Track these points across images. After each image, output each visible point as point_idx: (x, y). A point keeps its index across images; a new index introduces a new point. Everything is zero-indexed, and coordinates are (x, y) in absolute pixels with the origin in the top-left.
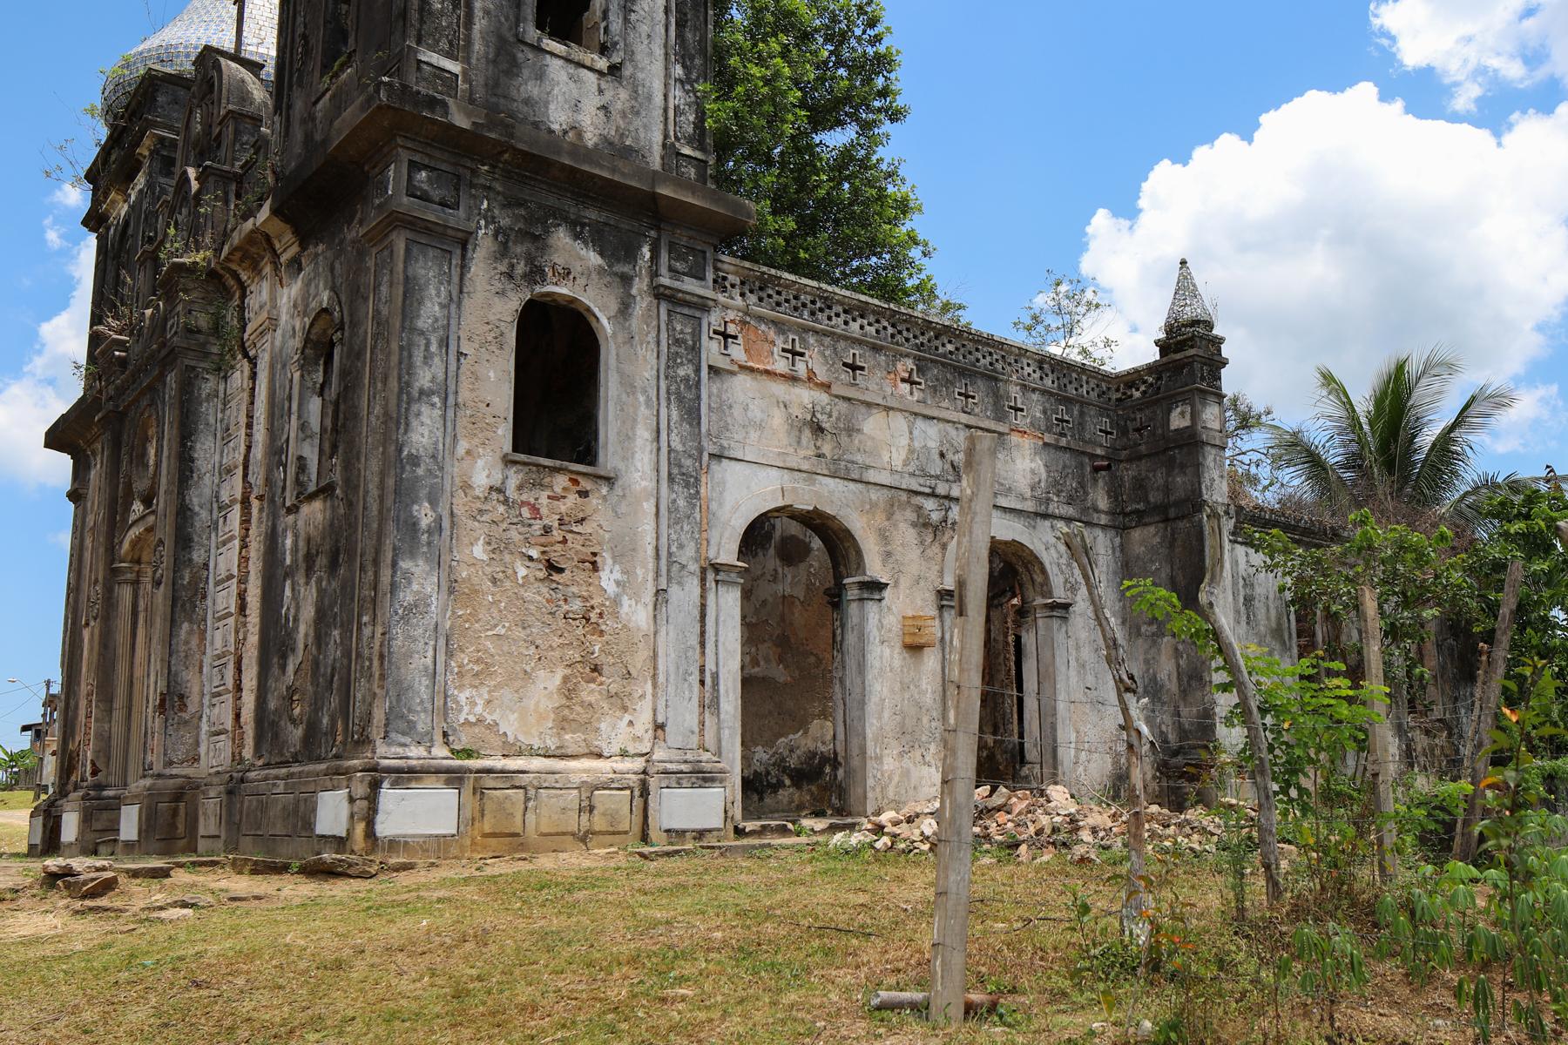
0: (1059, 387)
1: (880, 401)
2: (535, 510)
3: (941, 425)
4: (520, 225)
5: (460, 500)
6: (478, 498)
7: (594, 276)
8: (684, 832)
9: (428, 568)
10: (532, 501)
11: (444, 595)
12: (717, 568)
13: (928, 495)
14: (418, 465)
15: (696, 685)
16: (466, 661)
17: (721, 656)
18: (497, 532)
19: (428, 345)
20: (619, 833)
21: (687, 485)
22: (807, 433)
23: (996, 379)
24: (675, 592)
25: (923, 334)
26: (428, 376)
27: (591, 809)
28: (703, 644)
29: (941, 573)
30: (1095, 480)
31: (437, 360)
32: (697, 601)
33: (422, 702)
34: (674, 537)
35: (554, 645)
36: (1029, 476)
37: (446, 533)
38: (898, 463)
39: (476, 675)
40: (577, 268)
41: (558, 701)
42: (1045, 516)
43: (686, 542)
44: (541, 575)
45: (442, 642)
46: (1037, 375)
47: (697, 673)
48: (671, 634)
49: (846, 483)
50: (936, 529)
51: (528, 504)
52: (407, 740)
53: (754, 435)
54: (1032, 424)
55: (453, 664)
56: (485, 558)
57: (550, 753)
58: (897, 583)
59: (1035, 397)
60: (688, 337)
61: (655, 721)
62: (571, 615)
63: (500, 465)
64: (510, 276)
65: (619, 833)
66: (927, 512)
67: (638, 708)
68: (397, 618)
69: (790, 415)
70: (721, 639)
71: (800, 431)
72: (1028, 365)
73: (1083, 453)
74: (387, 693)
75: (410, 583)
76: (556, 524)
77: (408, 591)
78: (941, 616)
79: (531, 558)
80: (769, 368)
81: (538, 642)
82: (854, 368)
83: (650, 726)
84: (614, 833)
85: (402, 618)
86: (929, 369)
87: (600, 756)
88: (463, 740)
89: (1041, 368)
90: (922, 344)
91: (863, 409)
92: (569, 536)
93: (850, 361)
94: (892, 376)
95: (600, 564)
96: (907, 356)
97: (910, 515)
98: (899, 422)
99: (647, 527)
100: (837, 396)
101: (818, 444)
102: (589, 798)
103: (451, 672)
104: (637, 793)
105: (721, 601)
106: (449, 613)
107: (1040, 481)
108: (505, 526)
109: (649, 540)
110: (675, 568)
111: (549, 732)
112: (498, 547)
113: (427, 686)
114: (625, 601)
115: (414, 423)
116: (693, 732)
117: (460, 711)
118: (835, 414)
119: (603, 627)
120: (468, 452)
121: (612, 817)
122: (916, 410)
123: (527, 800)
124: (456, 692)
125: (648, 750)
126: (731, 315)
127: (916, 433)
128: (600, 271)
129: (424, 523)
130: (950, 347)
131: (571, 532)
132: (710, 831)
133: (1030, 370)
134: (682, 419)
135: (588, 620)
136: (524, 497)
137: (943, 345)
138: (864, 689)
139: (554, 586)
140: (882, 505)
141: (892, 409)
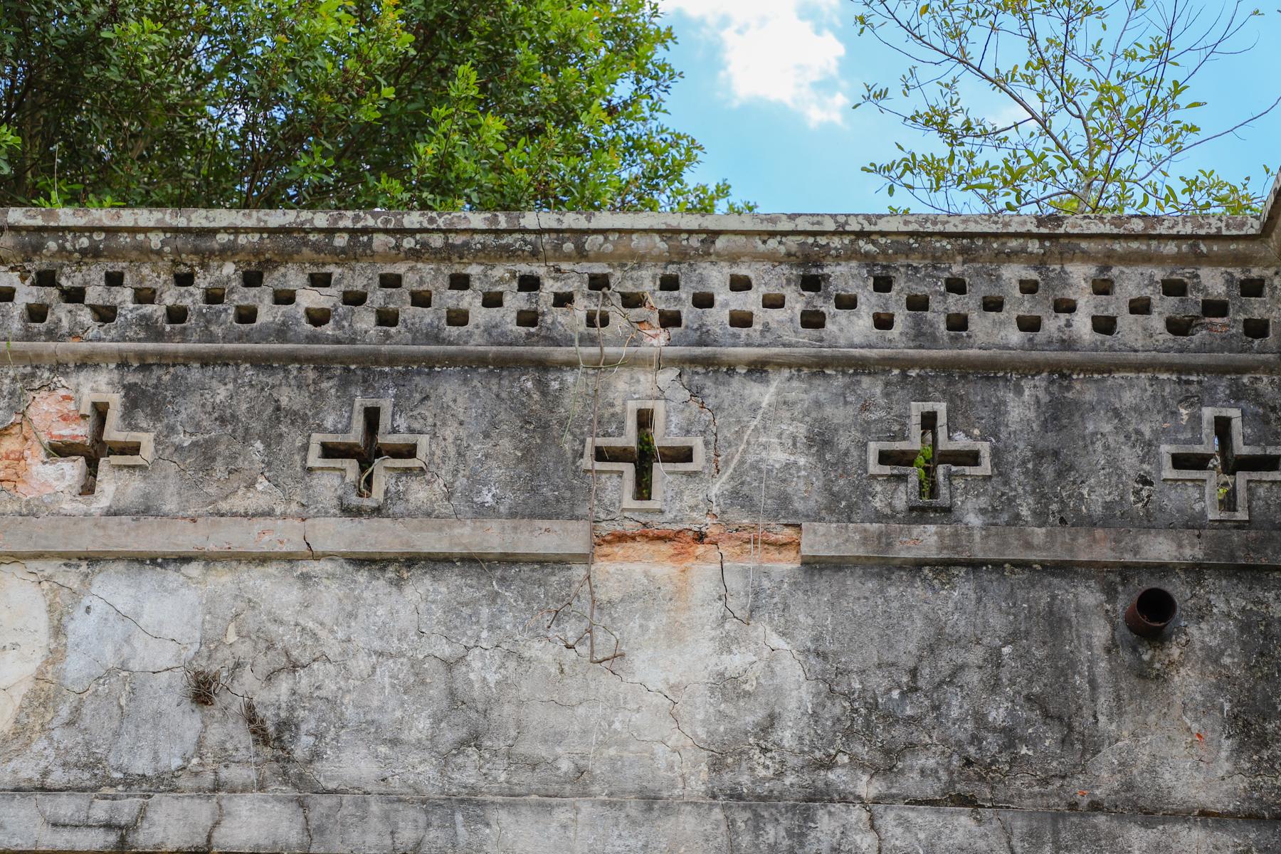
0: (921, 335)
3: (223, 579)
23: (543, 365)
25: (184, 280)
46: (797, 302)
54: (739, 497)
59: (765, 393)
72: (740, 284)
73: (1063, 569)
86: (181, 389)
89: (811, 284)
90: (177, 315)
96: (86, 363)
107: (772, 721)
122: (88, 542)
127: (81, 626)
130: (309, 298)
133: (750, 301)
137: (284, 298)
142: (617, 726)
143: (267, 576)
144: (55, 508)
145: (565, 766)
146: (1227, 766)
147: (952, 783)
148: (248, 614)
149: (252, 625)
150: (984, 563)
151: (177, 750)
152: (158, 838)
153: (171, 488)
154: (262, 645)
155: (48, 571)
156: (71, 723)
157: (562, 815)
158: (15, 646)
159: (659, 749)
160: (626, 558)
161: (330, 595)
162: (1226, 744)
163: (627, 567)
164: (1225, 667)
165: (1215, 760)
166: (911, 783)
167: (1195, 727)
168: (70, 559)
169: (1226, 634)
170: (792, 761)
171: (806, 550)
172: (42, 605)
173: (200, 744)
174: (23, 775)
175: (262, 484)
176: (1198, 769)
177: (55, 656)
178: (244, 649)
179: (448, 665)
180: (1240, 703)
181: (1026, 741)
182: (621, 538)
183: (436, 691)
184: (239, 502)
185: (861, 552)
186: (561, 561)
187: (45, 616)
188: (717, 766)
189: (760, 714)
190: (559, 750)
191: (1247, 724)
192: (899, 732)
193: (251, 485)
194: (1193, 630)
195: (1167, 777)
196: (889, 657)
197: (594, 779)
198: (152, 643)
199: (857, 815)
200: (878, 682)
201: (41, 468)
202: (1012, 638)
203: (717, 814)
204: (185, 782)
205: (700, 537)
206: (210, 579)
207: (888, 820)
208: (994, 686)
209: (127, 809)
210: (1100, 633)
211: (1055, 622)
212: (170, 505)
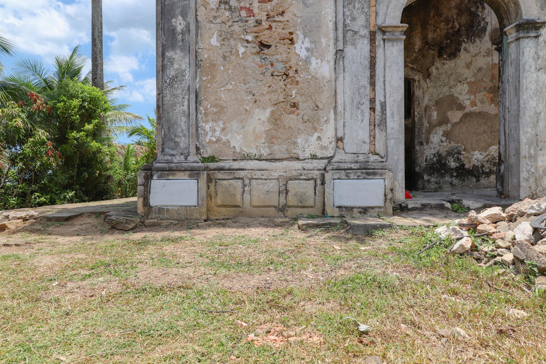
5: (202, 12)
6: (213, 9)
8: (352, 208)
9: (182, 54)
10: (248, 6)
11: (193, 69)
12: (383, 30)
15: (367, 112)
16: (209, 106)
17: (387, 91)
18: (225, 28)
20: (307, 207)
24: (349, 50)
27: (287, 192)
28: (373, 84)
32: (368, 55)
33: (182, 131)
34: (348, 13)
35: (265, 93)
37: (193, 32)
39: (216, 113)
41: (268, 126)
43: (357, 16)
44: (254, 51)
45: (193, 97)
47: (368, 103)
48: (347, 79)
51: (245, 8)
52: (175, 152)
55: (201, 108)
56: (218, 44)
57: (263, 158)
61: (336, 135)
62: (276, 73)
65: (307, 207)
67: (324, 128)
68: (166, 85)
70: (387, 79)
74: (162, 127)
75: (172, 64)
76: (265, 18)
77: (172, 69)
79: (248, 41)
81: (255, 92)
83: (334, 140)
84: (303, 207)
85: (168, 85)
87: (298, 159)
88: (207, 152)
95: (295, 40)
99: (328, 10)
102: (286, 185)
103: (201, 113)
104: (319, 182)
105: (387, 52)
106: (198, 79)
108: (230, 23)
109: (330, 18)
110: (349, 34)
111: (263, 145)
112: (225, 38)
113: (185, 122)
114: (314, 61)
116: (365, 143)
117: (206, 135)
119: (298, 79)
121: (302, 198)
123: (244, 186)
124: (204, 124)
125: (332, 155)
129: (179, 29)
131: (275, 21)
132: (372, 208)
135: (287, 75)
138: (519, 106)
139: (264, 57)
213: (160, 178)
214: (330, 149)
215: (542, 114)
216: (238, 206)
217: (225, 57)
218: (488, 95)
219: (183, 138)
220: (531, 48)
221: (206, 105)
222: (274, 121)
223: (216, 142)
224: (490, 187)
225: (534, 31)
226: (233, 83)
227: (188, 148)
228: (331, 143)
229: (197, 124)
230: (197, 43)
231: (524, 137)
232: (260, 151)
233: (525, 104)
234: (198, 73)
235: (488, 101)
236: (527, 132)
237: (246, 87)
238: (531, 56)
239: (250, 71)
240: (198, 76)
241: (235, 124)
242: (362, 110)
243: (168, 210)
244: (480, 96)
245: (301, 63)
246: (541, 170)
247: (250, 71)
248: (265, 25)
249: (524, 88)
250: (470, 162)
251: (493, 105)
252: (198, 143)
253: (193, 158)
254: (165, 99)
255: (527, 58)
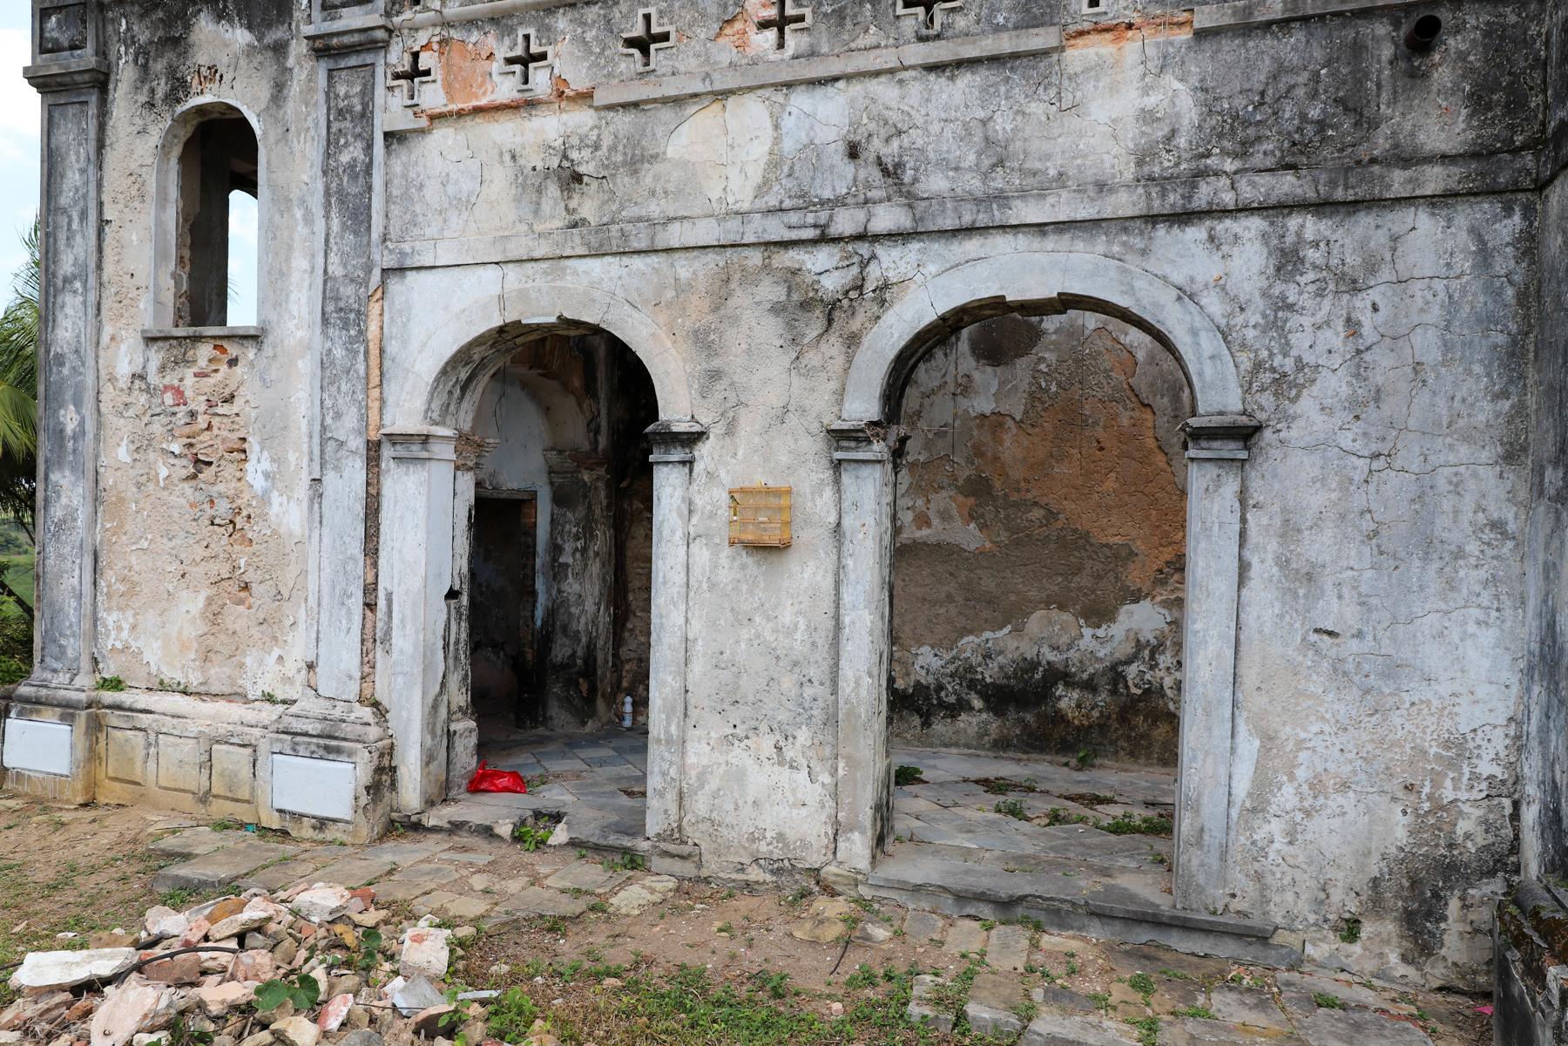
1: (698, 87)
2: (179, 393)
3: (857, 88)
4: (160, 33)
7: (243, 63)
9: (73, 479)
13: (814, 242)
14: (62, 364)
19: (69, 224)
21: (346, 326)
22: (553, 190)
26: (71, 259)
29: (840, 394)
30: (1417, 77)
31: (78, 238)
36: (1131, 134)
38: (742, 194)
40: (223, 62)
41: (202, 628)
42: (1183, 217)
44: (185, 473)
48: (325, 540)
49: (625, 260)
50: (831, 309)
53: (455, 221)
55: (103, 584)
56: (129, 460)
58: (731, 430)
60: (356, 101)
63: (142, 346)
64: (151, 105)
66: (809, 280)
69: (522, 169)
71: (539, 192)
78: (837, 481)
80: (483, 102)
81: (183, 556)
82: (642, 45)
91: (666, 114)
92: (216, 421)
93: (638, 31)
94: (738, 25)
97: (771, 291)
98: (751, 113)
100: (611, 108)
101: (573, 204)
106: (99, 526)
107: (1174, 133)
113: (75, 609)
115: (60, 317)
117: (108, 636)
118: (607, 141)
120: (113, 338)
126: (423, 37)
127: (788, 123)
128: (250, 51)
134: (344, 227)
136: (167, 381)
140: (702, 284)
141: (732, 92)
142: (1081, 146)
143: (881, 83)
144: (766, 59)
145: (1052, 172)
146: (1463, 126)
147: (1283, 157)
148: (872, 106)
149: (875, 113)
150: (1313, 16)
151: (844, 185)
152: (840, 230)
153: (824, 39)
154: (881, 123)
155: (767, 95)
156: (789, 175)
157: (1051, 200)
158: (757, 137)
159: (1106, 157)
160: (1085, 46)
161: (915, 89)
162: (1464, 112)
163: (1085, 51)
164: (1471, 62)
165: (1456, 123)
166: (1258, 160)
167: (1444, 104)
168: (778, 86)
169: (1474, 40)
170: (1185, 155)
171: (1197, 25)
172: (767, 114)
173: (855, 180)
174: (771, 204)
175: (873, 29)
176: (1443, 129)
177: (777, 140)
178: (872, 126)
179: (984, 122)
180: (1477, 85)
181: (1331, 127)
182: (1081, 34)
183: (978, 138)
184: (861, 42)
185: (1232, 21)
186: (1045, 53)
187: (769, 120)
188: (1140, 163)
189: (1166, 130)
190: (1048, 164)
191: (1479, 98)
192: (1251, 131)
193: (866, 31)
194: (1451, 42)
195: (1422, 137)
196: (1247, 86)
197: (1069, 178)
198: (825, 128)
199: (1224, 182)
200: (1240, 102)
201: (756, 37)
202: (1328, 63)
203: (1140, 190)
204: (850, 200)
205: (1130, 26)
206: (850, 89)
207: (1243, 184)
208: (1313, 96)
209: (823, 216)
210: (1387, 52)
211: (1357, 49)
212: (825, 49)
213: (20, 715)
214: (298, 683)
215: (700, 642)
216: (139, 784)
217: (139, 485)
218: (961, 498)
219: (72, 640)
220: (675, 489)
221: (109, 577)
222: (211, 616)
223: (122, 651)
224: (957, 745)
225: (679, 448)
226: (150, 537)
227: (77, 659)
228: (299, 671)
229: (95, 613)
230: (97, 457)
231: (657, 694)
232: (187, 677)
233: (661, 617)
234: (99, 515)
235: (961, 515)
236: (664, 683)
237: (171, 544)
238: (675, 506)
239: (176, 515)
240: (99, 521)
241: (150, 619)
242: (349, 609)
243: (29, 776)
244: (941, 500)
245: (254, 503)
246: (693, 773)
247: (176, 515)
248: (202, 421)
249: (661, 580)
250: (908, 674)
251: (972, 525)
252: (95, 650)
253: (84, 680)
254: (48, 562)
255: (667, 511)
